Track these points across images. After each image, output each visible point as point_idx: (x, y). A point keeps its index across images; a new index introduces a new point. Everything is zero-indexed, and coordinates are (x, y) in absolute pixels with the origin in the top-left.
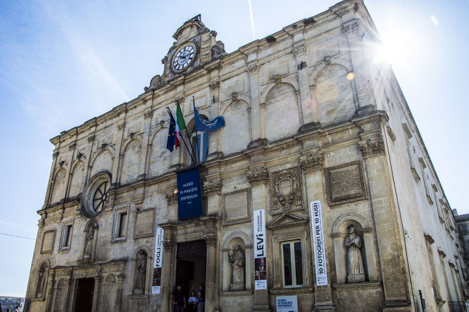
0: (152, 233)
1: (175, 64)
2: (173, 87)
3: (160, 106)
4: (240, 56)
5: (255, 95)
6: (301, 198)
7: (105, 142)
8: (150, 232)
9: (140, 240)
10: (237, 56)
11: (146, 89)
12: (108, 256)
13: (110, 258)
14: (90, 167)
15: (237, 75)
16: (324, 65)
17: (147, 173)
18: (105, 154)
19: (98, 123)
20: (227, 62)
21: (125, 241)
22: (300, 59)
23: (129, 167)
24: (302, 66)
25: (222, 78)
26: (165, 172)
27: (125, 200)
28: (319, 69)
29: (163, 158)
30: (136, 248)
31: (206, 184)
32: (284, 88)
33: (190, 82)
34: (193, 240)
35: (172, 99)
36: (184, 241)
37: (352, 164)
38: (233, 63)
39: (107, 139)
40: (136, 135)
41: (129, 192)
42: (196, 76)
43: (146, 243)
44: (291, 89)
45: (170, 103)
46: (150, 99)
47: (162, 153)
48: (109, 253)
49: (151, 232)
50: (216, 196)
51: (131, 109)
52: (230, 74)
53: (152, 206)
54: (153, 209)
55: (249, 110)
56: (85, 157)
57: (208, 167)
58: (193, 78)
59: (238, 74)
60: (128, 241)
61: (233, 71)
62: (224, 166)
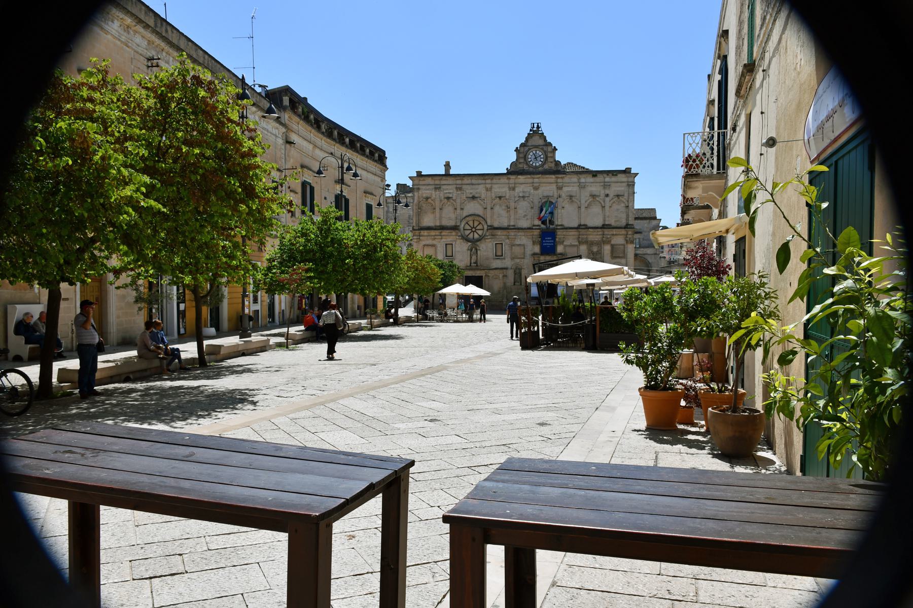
1: (529, 160)
5: (583, 201)
6: (601, 253)
8: (523, 256)
11: (507, 169)
14: (462, 209)
16: (616, 198)
21: (504, 259)
22: (607, 192)
24: (607, 195)
25: (565, 184)
28: (614, 200)
31: (557, 239)
32: (597, 202)
37: (622, 245)
40: (502, 198)
44: (600, 204)
53: (522, 243)
54: (524, 245)
55: (580, 207)
56: (455, 200)
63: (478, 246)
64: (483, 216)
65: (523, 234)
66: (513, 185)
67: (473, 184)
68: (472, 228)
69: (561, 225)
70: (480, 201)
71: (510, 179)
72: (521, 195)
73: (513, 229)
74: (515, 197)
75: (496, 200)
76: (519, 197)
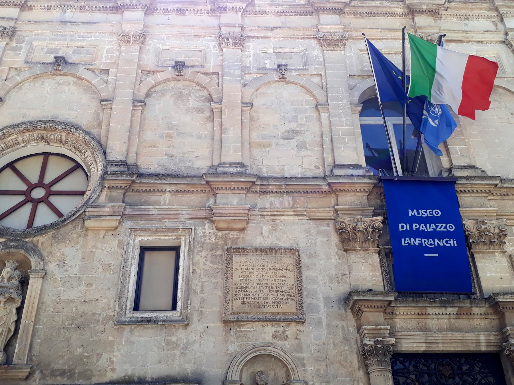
0: (296, 314)
2: (310, 9)
3: (269, 34)
4: (487, 13)
7: (60, 54)
8: (291, 308)
9: (248, 327)
10: (481, 9)
12: (103, 362)
13: (113, 370)
15: (478, 42)
17: (247, 163)
18: (59, 84)
19: (29, 4)
20: (454, 12)
23: (169, 136)
26: (309, 174)
27: (172, 213)
29: (294, 142)
30: (233, 347)
31: (469, 224)
33: (355, 14)
34: (452, 349)
35: (310, 33)
36: (423, 348)
38: (466, 17)
39: (70, 51)
40: (190, 70)
41: (178, 194)
42: (375, 10)
43: (274, 337)
45: (299, 38)
46: (235, 10)
47: (288, 131)
48: (105, 356)
49: (294, 311)
50: (498, 255)
51: (166, 11)
52: (464, 35)
57: (462, 189)
58: (367, 10)
59: (482, 42)
60: (196, 325)
61: (471, 32)
62: (496, 197)
63: (35, 250)
64: (95, 132)
65: (287, 199)
66: (238, 30)
67: (64, 23)
68: (32, 187)
69: (471, 167)
70: (88, 75)
71: (225, 9)
72: (270, 63)
73: (239, 174)
74: (244, 69)
75: (160, 77)
76: (263, 70)
